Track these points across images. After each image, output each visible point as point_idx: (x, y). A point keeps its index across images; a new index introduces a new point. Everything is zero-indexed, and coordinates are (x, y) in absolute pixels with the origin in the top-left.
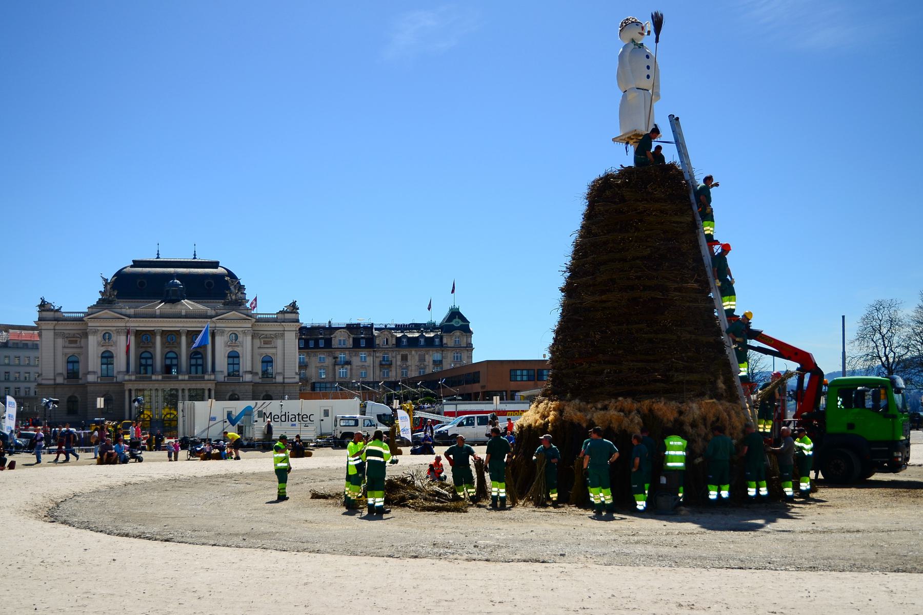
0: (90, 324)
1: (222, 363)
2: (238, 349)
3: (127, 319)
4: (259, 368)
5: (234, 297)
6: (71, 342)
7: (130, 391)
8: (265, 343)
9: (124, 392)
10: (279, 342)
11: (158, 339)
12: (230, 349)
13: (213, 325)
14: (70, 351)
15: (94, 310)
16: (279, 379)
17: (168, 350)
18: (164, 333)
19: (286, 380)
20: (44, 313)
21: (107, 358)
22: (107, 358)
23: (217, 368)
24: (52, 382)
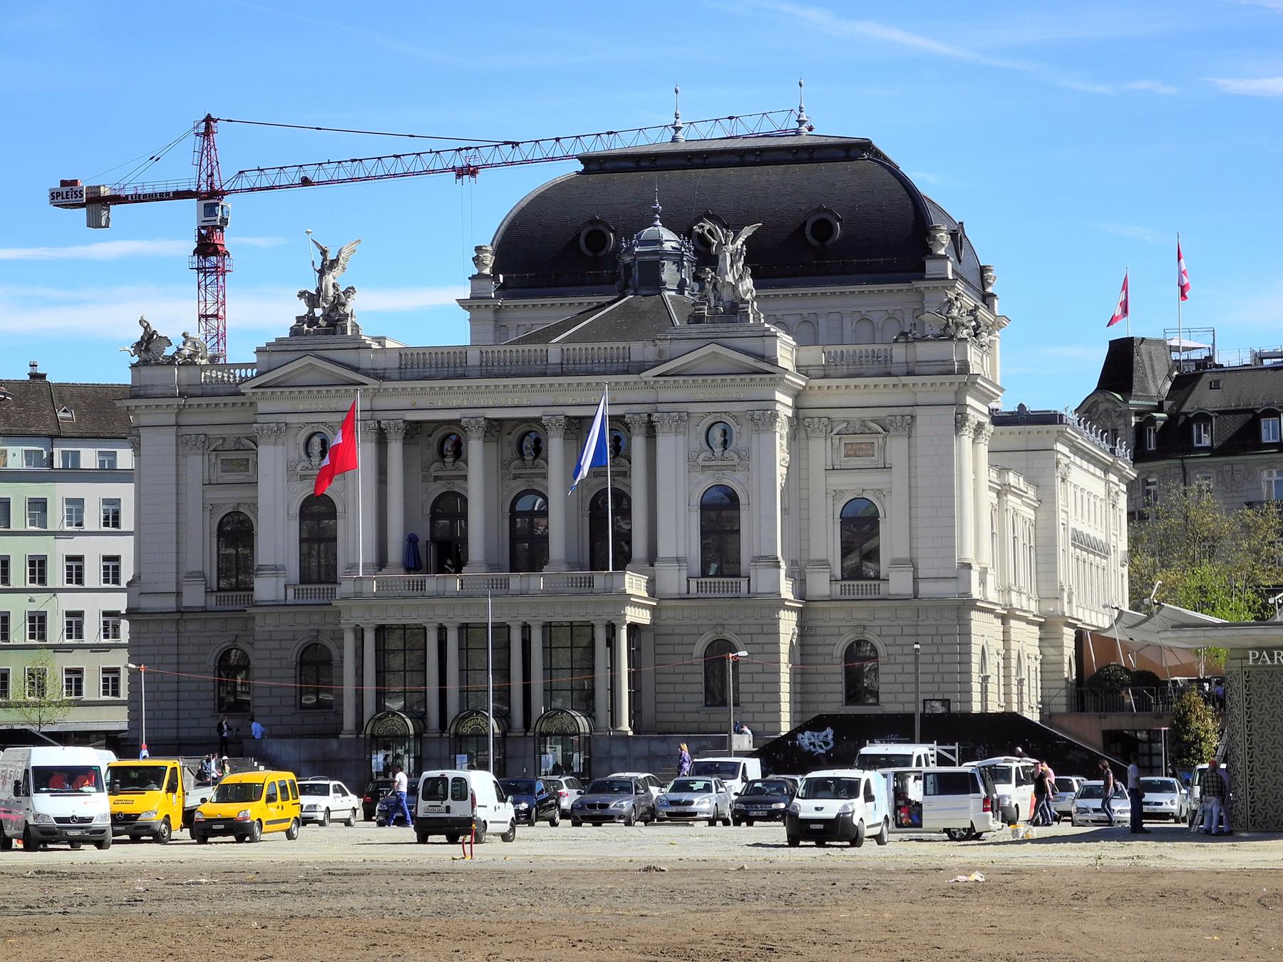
0: (262, 406)
1: (679, 533)
2: (731, 480)
3: (373, 384)
4: (827, 542)
5: (726, 295)
6: (229, 466)
7: (359, 633)
8: (852, 452)
9: (342, 631)
10: (896, 447)
11: (475, 448)
12: (705, 481)
13: (646, 395)
14: (228, 499)
15: (278, 358)
16: (899, 583)
17: (520, 486)
18: (494, 428)
20: (145, 371)
21: (318, 518)
22: (318, 518)
23: (664, 550)
24: (169, 603)
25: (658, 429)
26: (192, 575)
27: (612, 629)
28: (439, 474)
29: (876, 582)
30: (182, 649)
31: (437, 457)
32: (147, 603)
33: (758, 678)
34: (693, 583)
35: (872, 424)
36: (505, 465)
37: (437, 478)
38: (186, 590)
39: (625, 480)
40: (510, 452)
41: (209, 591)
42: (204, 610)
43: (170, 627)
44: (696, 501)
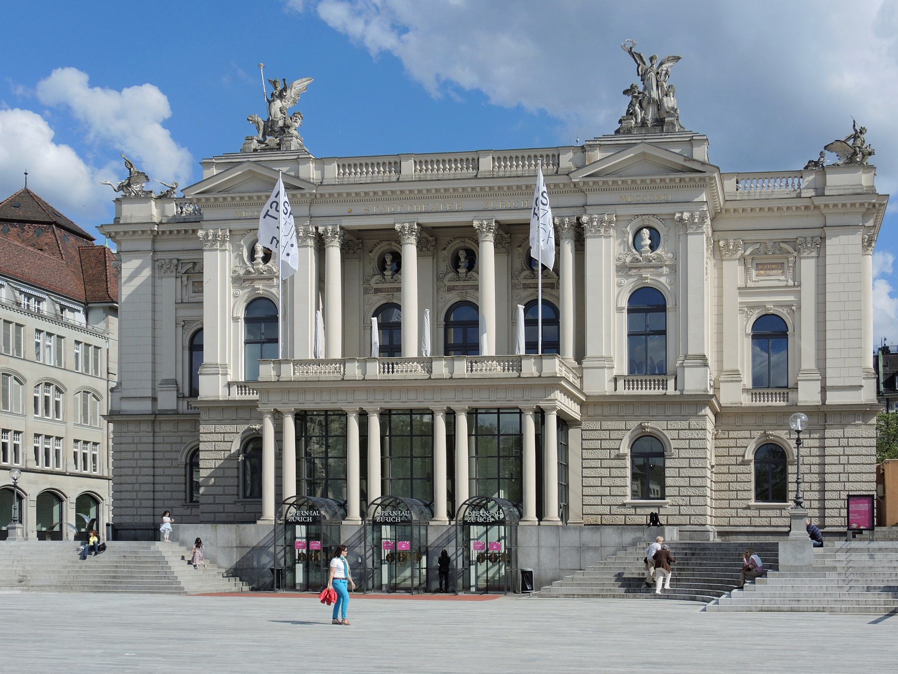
17: (453, 298)
19: (833, 399)
21: (263, 322)
24: (147, 406)
25: (588, 234)
26: (166, 382)
27: (540, 416)
28: (380, 286)
29: (785, 391)
30: (157, 447)
31: (377, 271)
32: (128, 407)
33: (684, 472)
34: (620, 383)
35: (782, 245)
36: (439, 278)
37: (377, 291)
38: (161, 396)
39: (554, 292)
40: (445, 265)
41: (180, 397)
42: (176, 412)
43: (146, 428)
44: (624, 304)
